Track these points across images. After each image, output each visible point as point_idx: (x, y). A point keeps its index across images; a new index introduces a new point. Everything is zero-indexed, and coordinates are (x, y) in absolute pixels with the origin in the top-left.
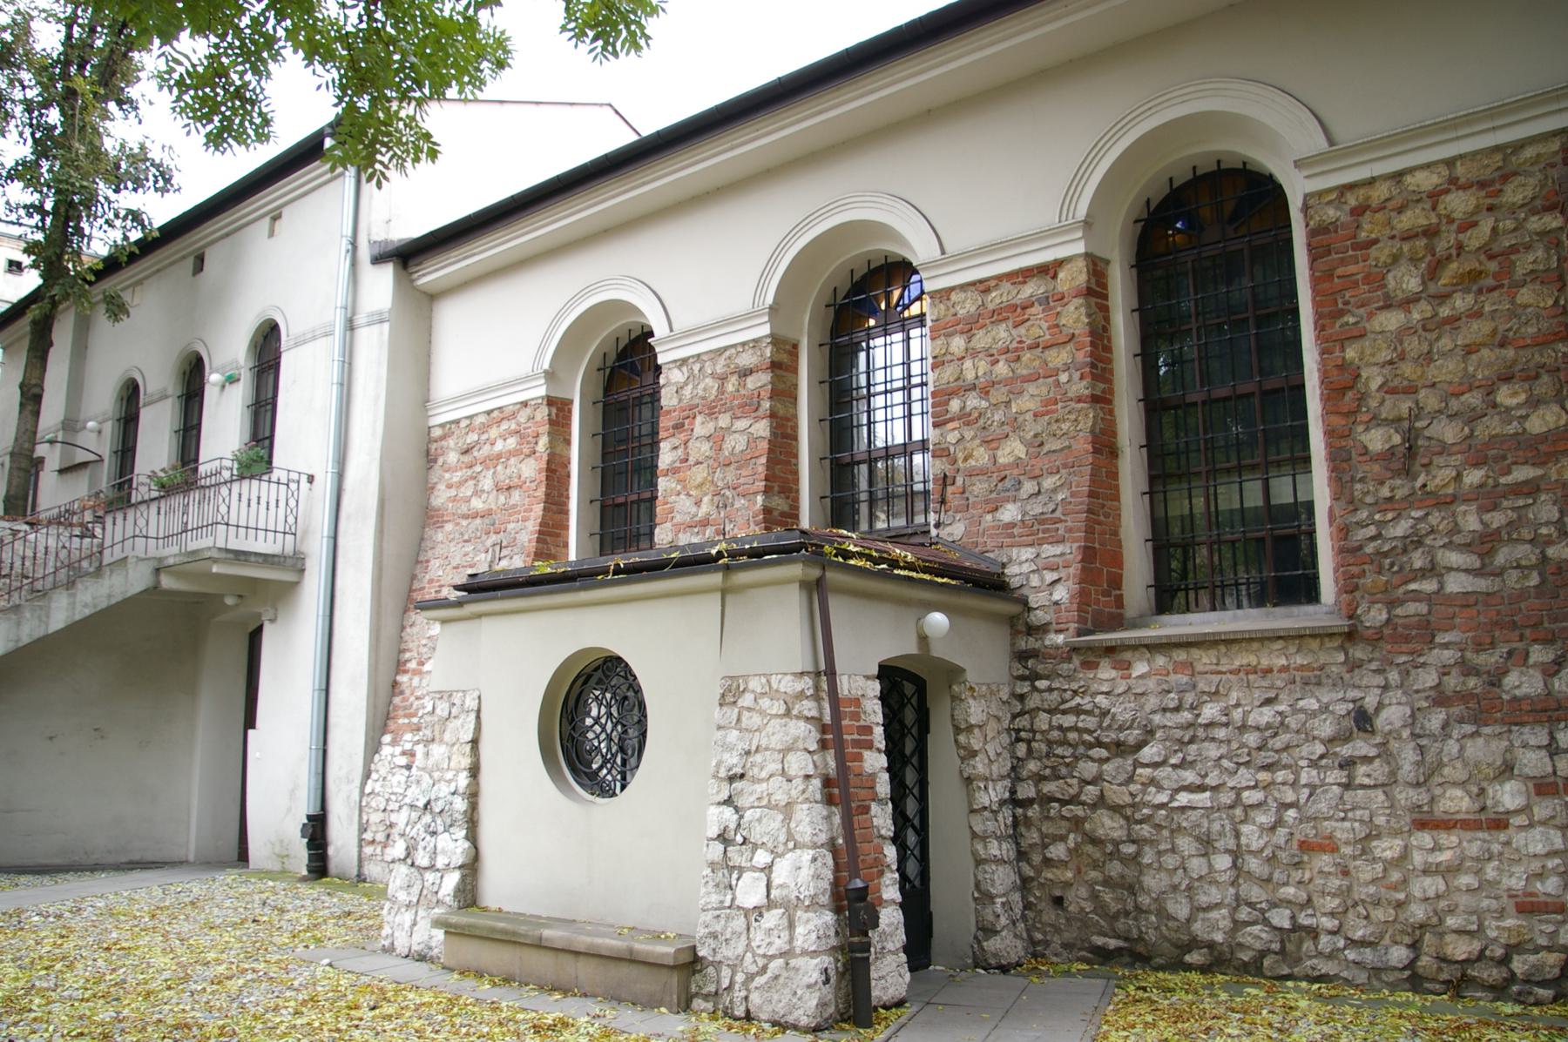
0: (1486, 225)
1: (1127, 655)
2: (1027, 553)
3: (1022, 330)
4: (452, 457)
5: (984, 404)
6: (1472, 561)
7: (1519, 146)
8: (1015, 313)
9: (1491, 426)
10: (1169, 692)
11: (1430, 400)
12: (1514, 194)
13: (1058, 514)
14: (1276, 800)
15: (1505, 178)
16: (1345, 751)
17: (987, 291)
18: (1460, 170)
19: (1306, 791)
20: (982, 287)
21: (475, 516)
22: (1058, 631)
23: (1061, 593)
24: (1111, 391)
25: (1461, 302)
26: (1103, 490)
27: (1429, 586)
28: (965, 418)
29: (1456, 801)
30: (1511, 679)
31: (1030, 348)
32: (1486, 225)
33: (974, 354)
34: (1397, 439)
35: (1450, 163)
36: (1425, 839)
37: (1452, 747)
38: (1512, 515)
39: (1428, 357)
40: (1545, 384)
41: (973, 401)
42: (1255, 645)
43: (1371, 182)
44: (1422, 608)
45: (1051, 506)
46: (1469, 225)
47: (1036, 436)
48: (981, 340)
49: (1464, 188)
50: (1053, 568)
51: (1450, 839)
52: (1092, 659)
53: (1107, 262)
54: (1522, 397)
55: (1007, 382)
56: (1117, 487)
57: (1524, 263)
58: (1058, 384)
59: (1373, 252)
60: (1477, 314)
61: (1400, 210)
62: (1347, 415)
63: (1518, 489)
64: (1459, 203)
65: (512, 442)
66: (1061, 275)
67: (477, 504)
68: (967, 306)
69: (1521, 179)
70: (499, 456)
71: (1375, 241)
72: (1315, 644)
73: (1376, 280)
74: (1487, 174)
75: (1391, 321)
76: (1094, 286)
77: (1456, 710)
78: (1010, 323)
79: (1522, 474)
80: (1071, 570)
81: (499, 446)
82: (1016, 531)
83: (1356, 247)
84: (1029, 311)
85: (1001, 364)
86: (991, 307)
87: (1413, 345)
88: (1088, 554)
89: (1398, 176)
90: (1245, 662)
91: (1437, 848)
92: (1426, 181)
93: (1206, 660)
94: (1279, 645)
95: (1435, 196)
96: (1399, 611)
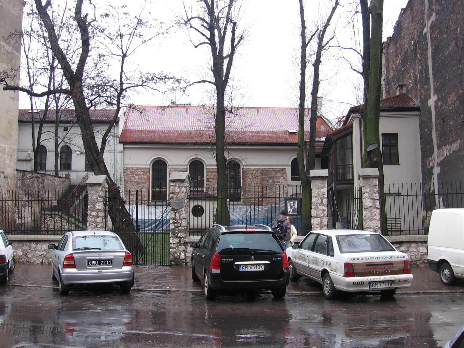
4: (129, 173)
12: (258, 172)
21: (134, 182)
25: (254, 180)
28: (211, 182)
41: (212, 180)
48: (213, 174)
57: (259, 178)
64: (255, 172)
65: (142, 173)
67: (134, 180)
68: (211, 170)
70: (139, 174)
75: (249, 180)
81: (139, 173)
92: (253, 169)
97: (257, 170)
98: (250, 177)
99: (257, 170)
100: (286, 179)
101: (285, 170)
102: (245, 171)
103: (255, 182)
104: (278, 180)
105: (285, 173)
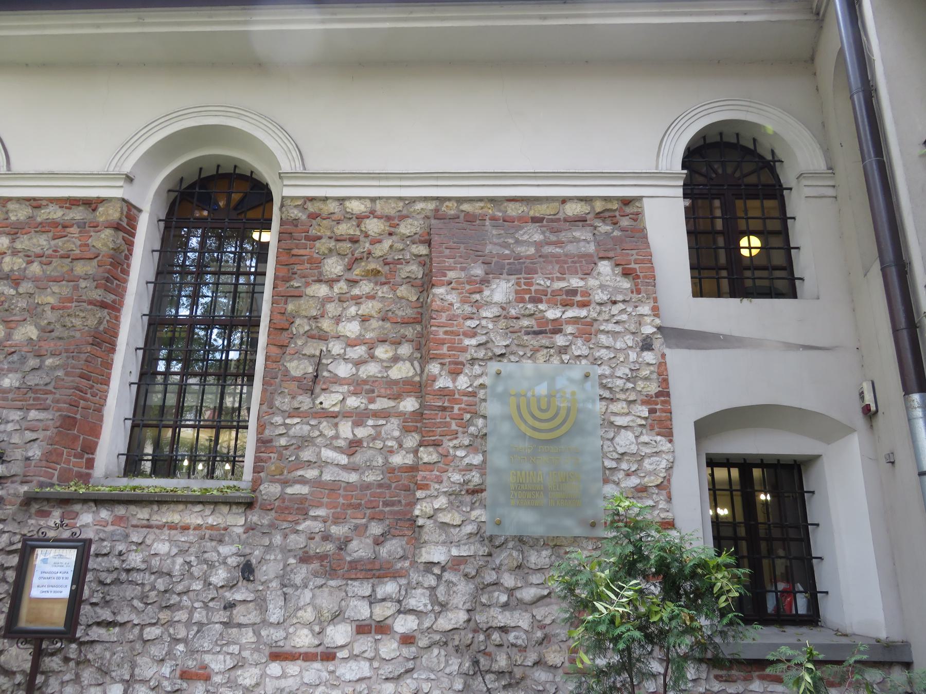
0: (387, 244)
1: (77, 507)
2: (16, 415)
3: (60, 242)
5: (12, 292)
6: (343, 460)
7: (414, 200)
8: (58, 228)
9: (371, 370)
10: (103, 540)
11: (336, 348)
12: (406, 228)
13: (50, 388)
14: (170, 635)
15: (403, 218)
16: (229, 596)
17: (38, 207)
18: (378, 206)
19: (195, 628)
20: (35, 204)
22: (22, 483)
23: (35, 452)
24: (121, 304)
26: (96, 375)
27: (311, 474)
29: (303, 640)
30: (354, 545)
31: (62, 257)
32: (387, 244)
33: (15, 252)
34: (310, 369)
35: (373, 200)
36: (275, 668)
37: (307, 595)
38: (372, 431)
39: (338, 320)
40: (405, 350)
42: (181, 507)
43: (326, 199)
44: (304, 490)
45: (47, 380)
46: (377, 241)
47: (49, 323)
48: (23, 243)
49: (379, 218)
50: (32, 430)
51: (293, 668)
52: (46, 508)
53: (140, 211)
54: (390, 354)
55: (35, 280)
56: (110, 374)
58: (76, 288)
59: (317, 244)
60: (371, 297)
61: (338, 222)
62: (282, 346)
63: (376, 414)
66: (101, 209)
68: (19, 214)
69: (410, 221)
71: (320, 238)
72: (225, 509)
73: (316, 263)
74: (392, 213)
75: (322, 290)
76: (124, 224)
77: (315, 565)
78: (50, 234)
79: (381, 404)
80: (48, 433)
82: (10, 396)
83: (307, 238)
84: (68, 230)
85: (35, 264)
86: (39, 219)
87: (332, 308)
88: (68, 422)
89: (342, 200)
90: (170, 520)
91: (284, 676)
92: (356, 207)
93: (140, 516)
94: (198, 508)
95: (360, 218)
96: (289, 491)
97: (390, 209)
98: (333, 266)
99: (396, 214)
100: (639, 274)
101: (637, 216)
102: (295, 222)
103: (369, 307)
104: (575, 282)
105: (638, 235)
